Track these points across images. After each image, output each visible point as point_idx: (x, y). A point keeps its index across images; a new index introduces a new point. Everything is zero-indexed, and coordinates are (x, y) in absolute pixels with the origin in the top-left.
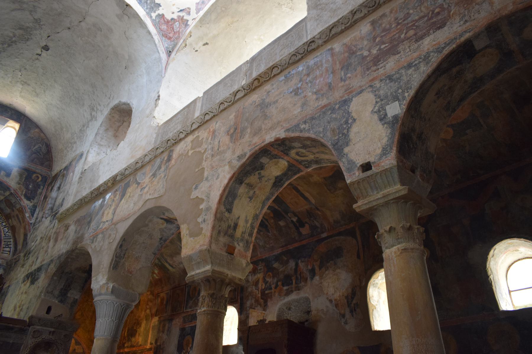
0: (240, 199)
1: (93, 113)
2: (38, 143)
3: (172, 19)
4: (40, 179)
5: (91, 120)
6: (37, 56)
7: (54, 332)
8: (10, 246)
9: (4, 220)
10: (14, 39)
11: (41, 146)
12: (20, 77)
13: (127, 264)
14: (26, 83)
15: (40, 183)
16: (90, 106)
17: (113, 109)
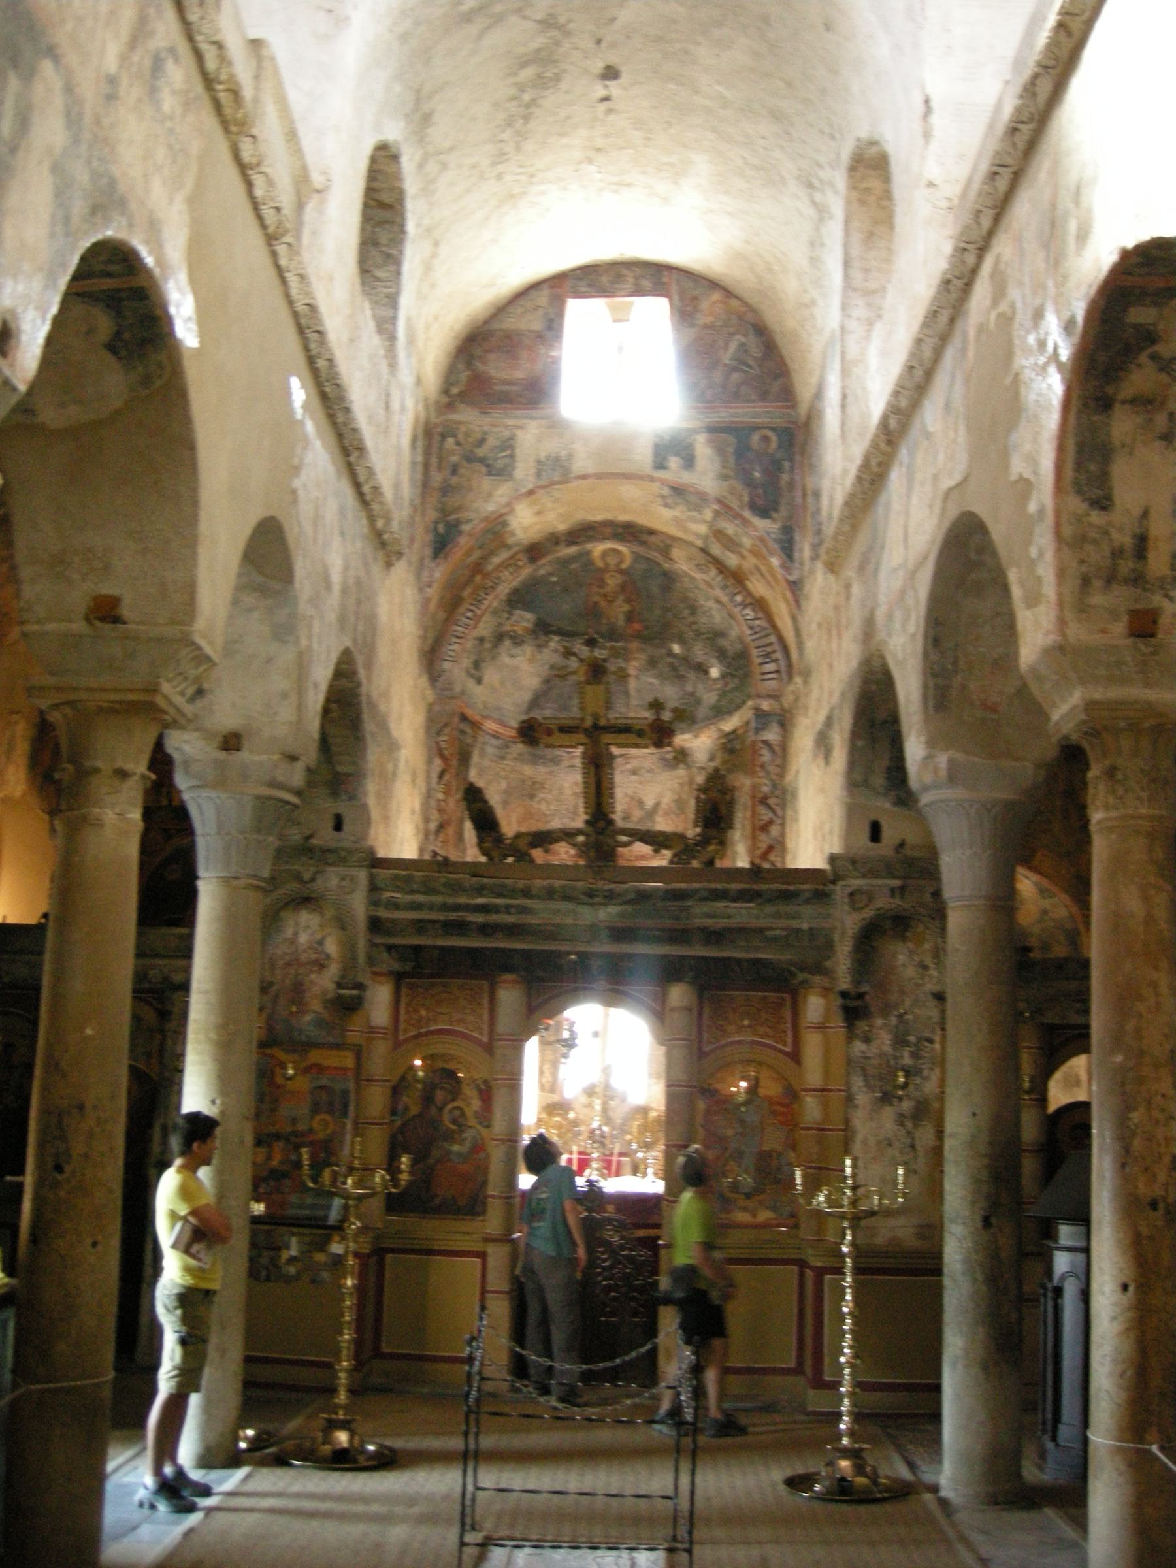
0: (1131, 454)
1: (818, 197)
2: (732, 334)
4: (774, 444)
5: (821, 220)
6: (606, 104)
7: (902, 889)
8: (774, 656)
10: (526, 97)
11: (743, 340)
12: (599, 176)
13: (972, 687)
14: (620, 184)
15: (779, 455)
16: (798, 178)
17: (852, 169)
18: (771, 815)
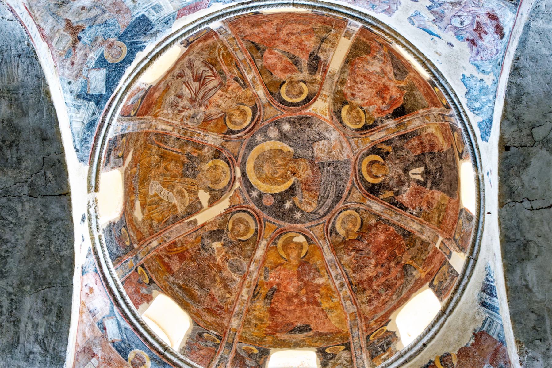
3: (460, 38)
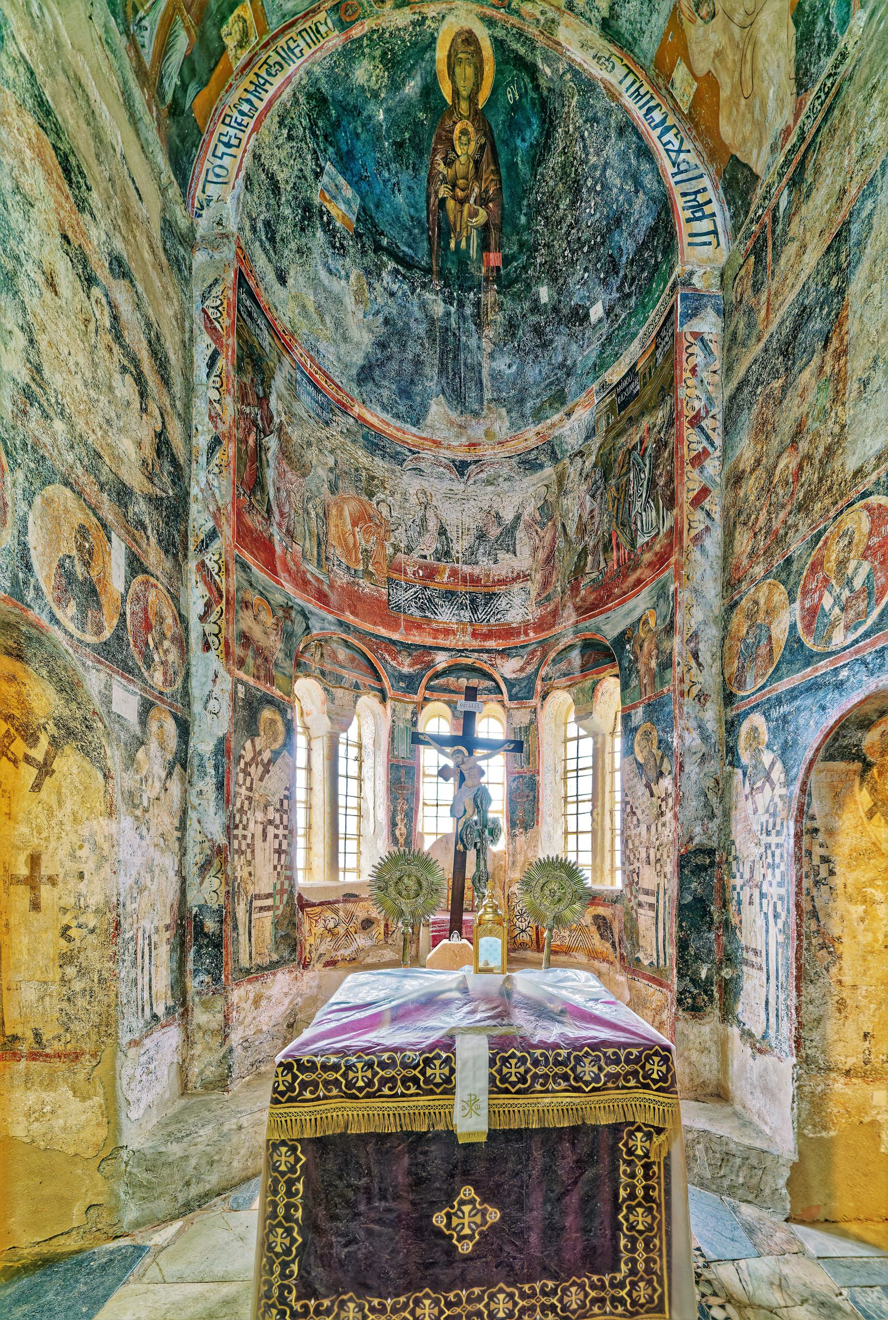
8: (707, 210)
9: (652, 98)
18: (705, 443)
